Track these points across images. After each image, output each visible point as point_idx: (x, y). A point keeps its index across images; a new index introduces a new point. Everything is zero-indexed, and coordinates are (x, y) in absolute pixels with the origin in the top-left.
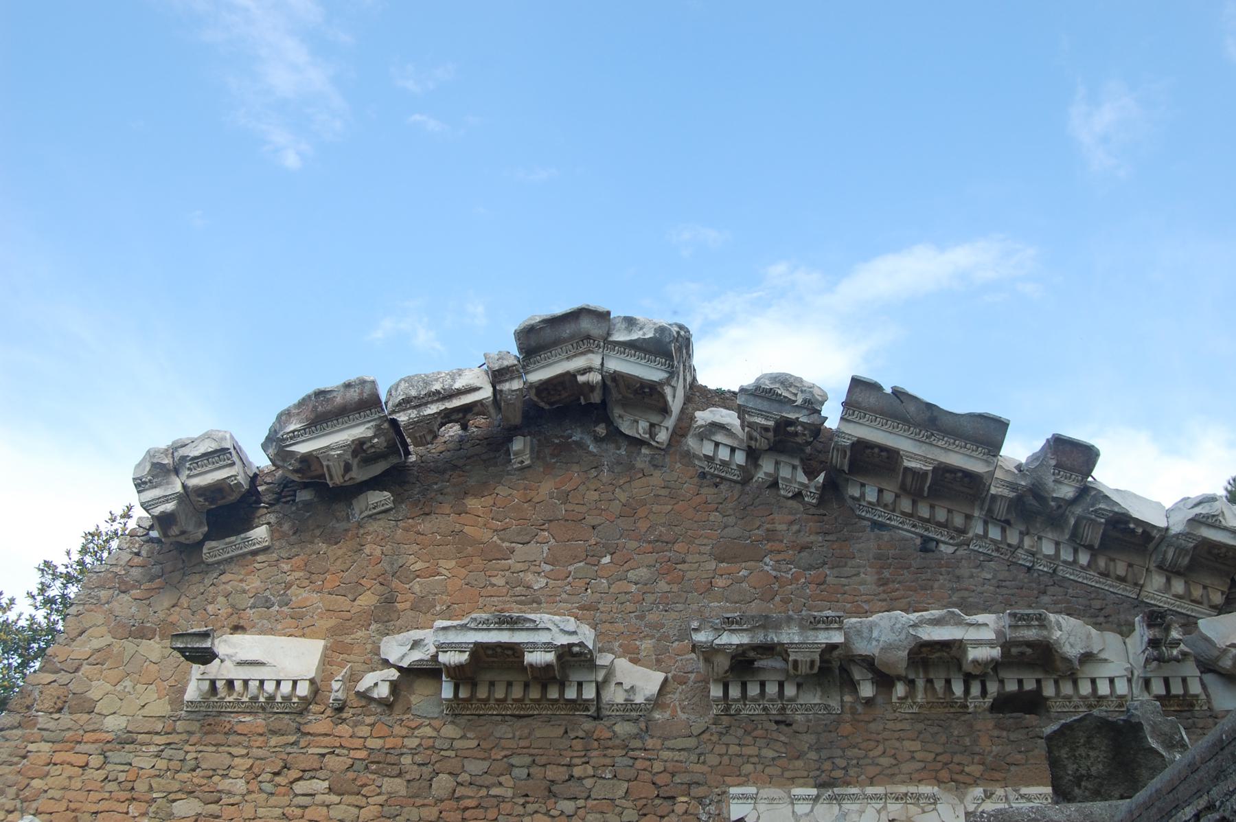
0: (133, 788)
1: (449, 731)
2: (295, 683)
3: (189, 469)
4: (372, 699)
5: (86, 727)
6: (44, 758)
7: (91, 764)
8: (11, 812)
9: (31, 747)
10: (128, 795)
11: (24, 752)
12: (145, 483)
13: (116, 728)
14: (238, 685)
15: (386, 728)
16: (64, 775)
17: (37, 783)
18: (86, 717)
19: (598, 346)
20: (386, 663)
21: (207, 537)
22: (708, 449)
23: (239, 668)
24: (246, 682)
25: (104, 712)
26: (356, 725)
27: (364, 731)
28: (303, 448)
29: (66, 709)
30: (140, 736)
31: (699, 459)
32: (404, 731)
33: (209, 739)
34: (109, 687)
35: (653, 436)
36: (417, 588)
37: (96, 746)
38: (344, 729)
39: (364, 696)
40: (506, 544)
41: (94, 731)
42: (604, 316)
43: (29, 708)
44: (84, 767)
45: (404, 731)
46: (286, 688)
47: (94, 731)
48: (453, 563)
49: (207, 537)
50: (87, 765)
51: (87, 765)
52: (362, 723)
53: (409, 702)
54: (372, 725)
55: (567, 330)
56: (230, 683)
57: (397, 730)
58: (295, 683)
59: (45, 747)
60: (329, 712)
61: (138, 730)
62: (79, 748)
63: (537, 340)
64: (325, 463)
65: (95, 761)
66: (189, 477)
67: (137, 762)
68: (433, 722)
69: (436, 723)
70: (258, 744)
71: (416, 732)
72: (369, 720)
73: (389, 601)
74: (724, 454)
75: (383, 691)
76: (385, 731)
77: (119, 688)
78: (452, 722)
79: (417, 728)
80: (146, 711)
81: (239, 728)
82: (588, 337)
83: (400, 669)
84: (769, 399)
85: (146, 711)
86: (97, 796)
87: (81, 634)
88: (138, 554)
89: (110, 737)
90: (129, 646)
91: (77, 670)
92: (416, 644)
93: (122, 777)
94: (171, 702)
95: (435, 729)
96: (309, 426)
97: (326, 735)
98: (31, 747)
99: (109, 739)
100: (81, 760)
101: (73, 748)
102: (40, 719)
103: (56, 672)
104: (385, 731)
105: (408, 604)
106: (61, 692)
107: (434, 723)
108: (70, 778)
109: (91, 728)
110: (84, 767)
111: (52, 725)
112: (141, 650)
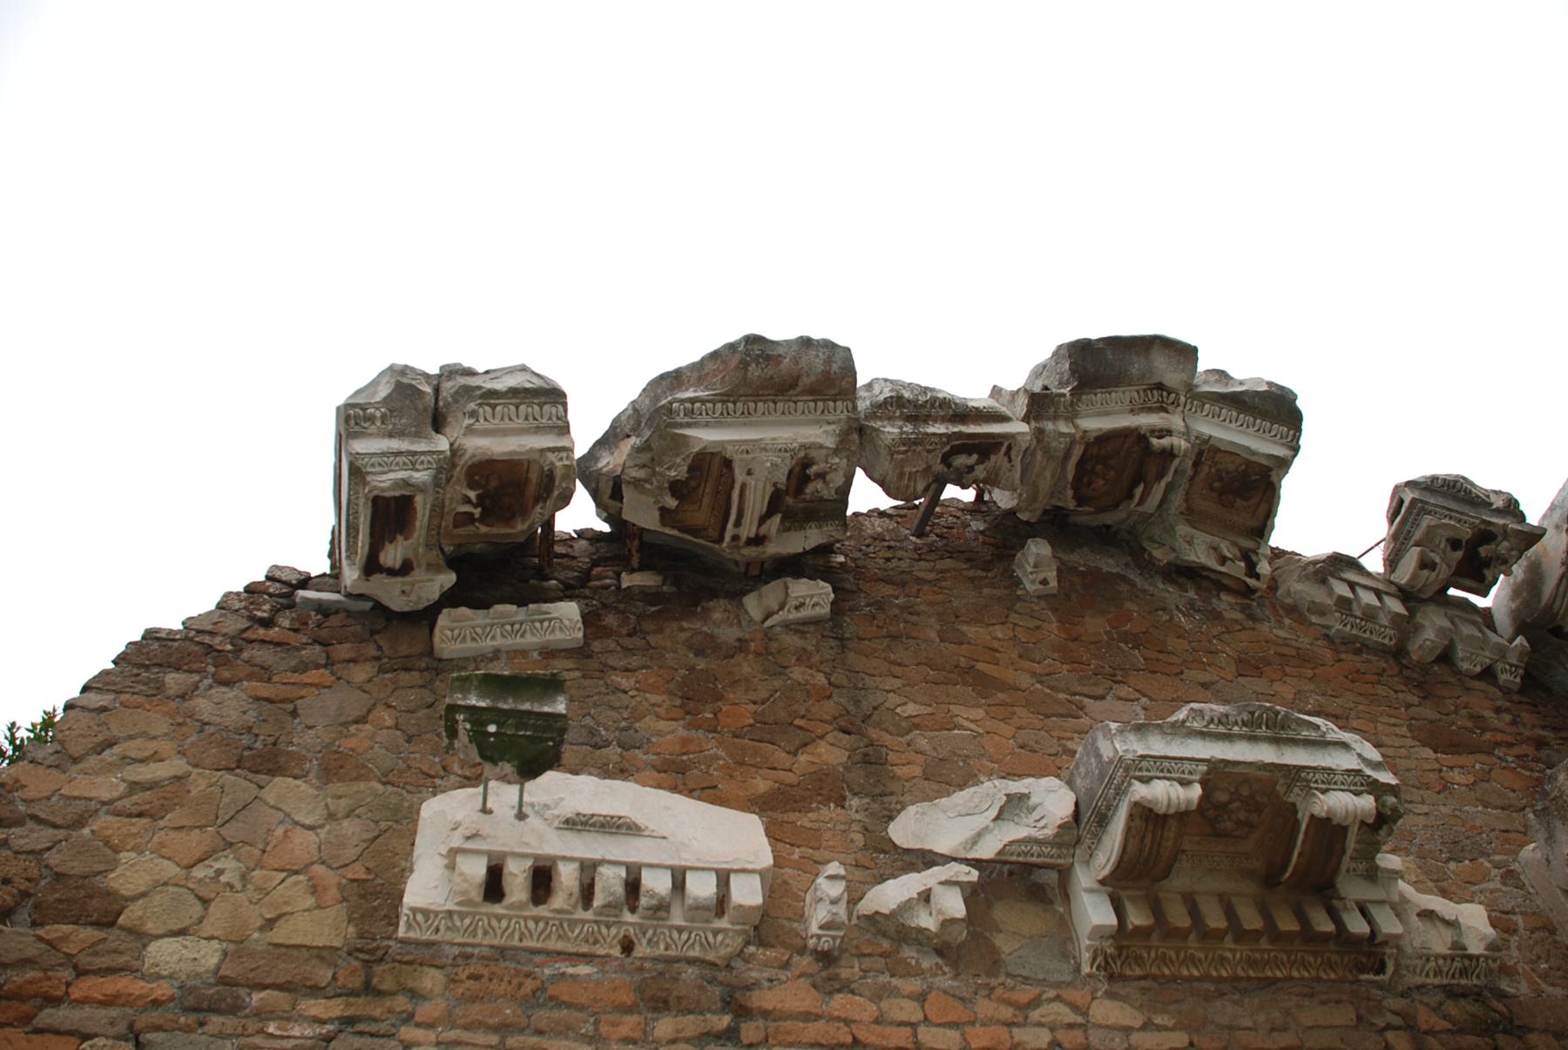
1: (1107, 1011)
2: (724, 878)
3: (473, 414)
4: (919, 937)
5: (84, 960)
12: (371, 419)
13: (187, 967)
14: (567, 876)
15: (957, 1003)
18: (88, 933)
19: (1176, 403)
20: (925, 859)
21: (450, 599)
22: (1342, 590)
23: (569, 835)
24: (589, 869)
25: (150, 927)
26: (877, 997)
27: (908, 1010)
28: (706, 436)
31: (1321, 611)
32: (1007, 1013)
33: (475, 1011)
34: (171, 870)
35: (1252, 570)
36: (923, 743)
38: (839, 1003)
39: (891, 931)
40: (1062, 696)
42: (1187, 353)
45: (1007, 1013)
46: (701, 887)
48: (979, 713)
49: (450, 599)
52: (894, 992)
53: (994, 951)
54: (921, 998)
55: (1136, 366)
56: (542, 879)
57: (985, 1007)
58: (724, 878)
60: (804, 962)
63: (1095, 364)
64: (740, 476)
66: (470, 431)
68: (1067, 994)
69: (1077, 996)
70: (624, 1030)
71: (1035, 1015)
72: (914, 985)
73: (872, 760)
74: (1368, 598)
75: (954, 904)
76: (957, 1012)
77: (199, 872)
78: (1111, 995)
79: (1035, 1003)
81: (563, 991)
82: (1160, 386)
83: (976, 863)
84: (1455, 498)
85: (280, 934)
87: (100, 748)
88: (267, 623)
89: (163, 990)
90: (238, 785)
91: (79, 822)
92: (1014, 805)
94: (359, 917)
95: (1075, 1008)
96: (728, 397)
97: (808, 1017)
99: (158, 994)
104: (957, 1012)
105: (918, 771)
107: (1067, 994)
112: (270, 794)
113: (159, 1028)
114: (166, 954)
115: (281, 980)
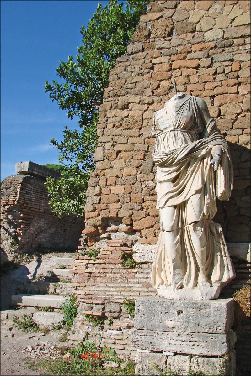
0: (238, 77)
5: (192, 41)
6: (166, 67)
7: (202, 65)
8: (149, 104)
9: (154, 61)
10: (236, 81)
11: (151, 65)
13: (216, 38)
16: (184, 74)
17: (163, 83)
29: (174, 33)
30: (235, 41)
37: (203, 52)
41: (198, 43)
43: (148, 36)
44: (197, 67)
47: (198, 43)
50: (199, 65)
51: (199, 65)
59: (165, 59)
61: (234, 36)
62: (189, 56)
65: (205, 62)
67: (236, 58)
80: (234, 24)
86: (213, 85)
93: (228, 70)
98: (154, 61)
100: (194, 63)
101: (185, 57)
102: (157, 43)
103: (161, 11)
106: (168, 22)
108: (188, 76)
109: (196, 41)
110: (197, 67)
111: (166, 44)
113: (214, 54)
114: (209, 35)
115: (240, 36)
